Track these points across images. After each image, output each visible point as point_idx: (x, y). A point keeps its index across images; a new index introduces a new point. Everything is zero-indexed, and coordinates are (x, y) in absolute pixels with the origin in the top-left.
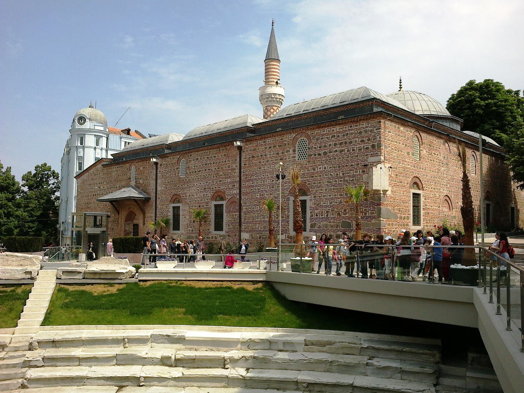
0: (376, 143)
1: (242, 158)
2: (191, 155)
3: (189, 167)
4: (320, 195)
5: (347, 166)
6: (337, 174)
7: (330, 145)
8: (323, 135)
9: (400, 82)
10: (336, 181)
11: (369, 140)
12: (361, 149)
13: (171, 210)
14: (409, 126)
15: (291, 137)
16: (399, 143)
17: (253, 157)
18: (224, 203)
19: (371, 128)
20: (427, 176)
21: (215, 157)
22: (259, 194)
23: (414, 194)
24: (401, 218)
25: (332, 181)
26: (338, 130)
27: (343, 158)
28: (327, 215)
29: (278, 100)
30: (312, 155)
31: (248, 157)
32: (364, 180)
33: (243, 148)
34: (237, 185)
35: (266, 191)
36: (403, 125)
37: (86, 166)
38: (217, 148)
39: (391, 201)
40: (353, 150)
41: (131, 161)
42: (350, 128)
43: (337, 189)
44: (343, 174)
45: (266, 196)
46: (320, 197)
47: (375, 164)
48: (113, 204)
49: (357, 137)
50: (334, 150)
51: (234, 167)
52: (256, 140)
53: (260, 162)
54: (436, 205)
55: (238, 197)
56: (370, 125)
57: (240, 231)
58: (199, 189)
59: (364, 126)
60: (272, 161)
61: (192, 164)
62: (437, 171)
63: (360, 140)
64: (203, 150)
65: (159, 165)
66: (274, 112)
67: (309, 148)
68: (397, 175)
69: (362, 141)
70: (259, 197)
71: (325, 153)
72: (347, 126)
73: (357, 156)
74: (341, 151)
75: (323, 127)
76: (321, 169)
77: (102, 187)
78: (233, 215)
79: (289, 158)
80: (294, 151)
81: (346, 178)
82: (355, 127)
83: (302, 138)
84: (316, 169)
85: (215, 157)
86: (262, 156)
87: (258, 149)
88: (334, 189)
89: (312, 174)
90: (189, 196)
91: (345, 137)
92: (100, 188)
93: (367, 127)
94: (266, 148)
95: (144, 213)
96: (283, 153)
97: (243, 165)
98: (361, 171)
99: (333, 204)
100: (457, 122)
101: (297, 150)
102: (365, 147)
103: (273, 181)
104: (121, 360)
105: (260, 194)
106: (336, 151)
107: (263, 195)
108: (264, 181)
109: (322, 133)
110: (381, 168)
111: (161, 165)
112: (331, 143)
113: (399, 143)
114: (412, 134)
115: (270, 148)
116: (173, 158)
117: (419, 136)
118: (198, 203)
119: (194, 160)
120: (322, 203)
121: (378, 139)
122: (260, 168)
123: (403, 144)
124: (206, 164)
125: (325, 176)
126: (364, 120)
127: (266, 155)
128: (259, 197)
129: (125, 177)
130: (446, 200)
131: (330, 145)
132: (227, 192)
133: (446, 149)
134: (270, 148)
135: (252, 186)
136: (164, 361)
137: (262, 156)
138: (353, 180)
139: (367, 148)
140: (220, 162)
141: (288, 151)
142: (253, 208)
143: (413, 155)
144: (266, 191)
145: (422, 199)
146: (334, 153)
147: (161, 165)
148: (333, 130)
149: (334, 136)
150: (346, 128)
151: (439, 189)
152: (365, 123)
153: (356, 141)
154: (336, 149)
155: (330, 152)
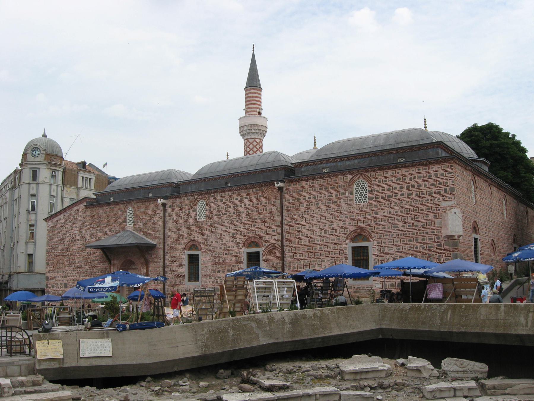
0: (448, 188)
1: (284, 200)
2: (213, 196)
3: (210, 210)
4: (385, 241)
5: (416, 210)
6: (405, 219)
8: (386, 177)
9: (425, 122)
10: (404, 226)
12: (431, 194)
13: (186, 259)
14: (469, 170)
15: (347, 179)
17: (298, 199)
19: (442, 172)
21: (246, 198)
25: (399, 226)
27: (411, 202)
29: (261, 132)
30: (373, 198)
31: (291, 199)
32: (437, 225)
33: (284, 189)
34: (278, 230)
37: (64, 207)
38: (249, 188)
40: (423, 194)
41: (128, 202)
42: (417, 171)
43: (406, 234)
44: (412, 219)
45: (316, 242)
46: (384, 243)
47: (448, 209)
49: (427, 181)
50: (400, 193)
51: (273, 210)
52: (302, 180)
53: (307, 205)
55: (280, 243)
56: (440, 169)
58: (225, 234)
59: (434, 169)
60: (324, 204)
61: (215, 206)
63: (430, 184)
64: (231, 190)
65: (167, 207)
66: (257, 145)
69: (433, 185)
70: (307, 243)
71: (389, 197)
72: (414, 169)
73: (428, 200)
74: (409, 195)
75: (385, 169)
76: (385, 214)
77: (84, 232)
78: (273, 264)
79: (345, 201)
81: (415, 223)
83: (360, 180)
84: (379, 213)
85: (246, 198)
86: (309, 198)
87: (305, 191)
88: (401, 235)
89: (375, 218)
90: (212, 242)
91: (413, 181)
92: (81, 232)
93: (437, 171)
94: (315, 190)
95: (147, 263)
96: (337, 195)
97: (285, 208)
98: (433, 216)
99: (401, 250)
100: (486, 164)
101: (354, 193)
102: (436, 191)
103: (325, 226)
105: (309, 241)
106: (402, 195)
107: (312, 241)
109: (385, 175)
112: (396, 186)
115: (320, 189)
116: (188, 199)
118: (224, 250)
121: (451, 183)
122: (308, 212)
124: (234, 207)
125: (390, 221)
126: (434, 163)
127: (315, 198)
128: (307, 243)
131: (395, 188)
132: (264, 238)
134: (320, 189)
135: (298, 232)
137: (309, 198)
138: (424, 225)
139: (439, 193)
140: (253, 204)
141: (343, 194)
142: (300, 256)
146: (400, 197)
147: (170, 207)
148: (398, 173)
149: (399, 179)
150: (413, 171)
152: (435, 167)
153: (425, 185)
154: (403, 192)
155: (395, 196)
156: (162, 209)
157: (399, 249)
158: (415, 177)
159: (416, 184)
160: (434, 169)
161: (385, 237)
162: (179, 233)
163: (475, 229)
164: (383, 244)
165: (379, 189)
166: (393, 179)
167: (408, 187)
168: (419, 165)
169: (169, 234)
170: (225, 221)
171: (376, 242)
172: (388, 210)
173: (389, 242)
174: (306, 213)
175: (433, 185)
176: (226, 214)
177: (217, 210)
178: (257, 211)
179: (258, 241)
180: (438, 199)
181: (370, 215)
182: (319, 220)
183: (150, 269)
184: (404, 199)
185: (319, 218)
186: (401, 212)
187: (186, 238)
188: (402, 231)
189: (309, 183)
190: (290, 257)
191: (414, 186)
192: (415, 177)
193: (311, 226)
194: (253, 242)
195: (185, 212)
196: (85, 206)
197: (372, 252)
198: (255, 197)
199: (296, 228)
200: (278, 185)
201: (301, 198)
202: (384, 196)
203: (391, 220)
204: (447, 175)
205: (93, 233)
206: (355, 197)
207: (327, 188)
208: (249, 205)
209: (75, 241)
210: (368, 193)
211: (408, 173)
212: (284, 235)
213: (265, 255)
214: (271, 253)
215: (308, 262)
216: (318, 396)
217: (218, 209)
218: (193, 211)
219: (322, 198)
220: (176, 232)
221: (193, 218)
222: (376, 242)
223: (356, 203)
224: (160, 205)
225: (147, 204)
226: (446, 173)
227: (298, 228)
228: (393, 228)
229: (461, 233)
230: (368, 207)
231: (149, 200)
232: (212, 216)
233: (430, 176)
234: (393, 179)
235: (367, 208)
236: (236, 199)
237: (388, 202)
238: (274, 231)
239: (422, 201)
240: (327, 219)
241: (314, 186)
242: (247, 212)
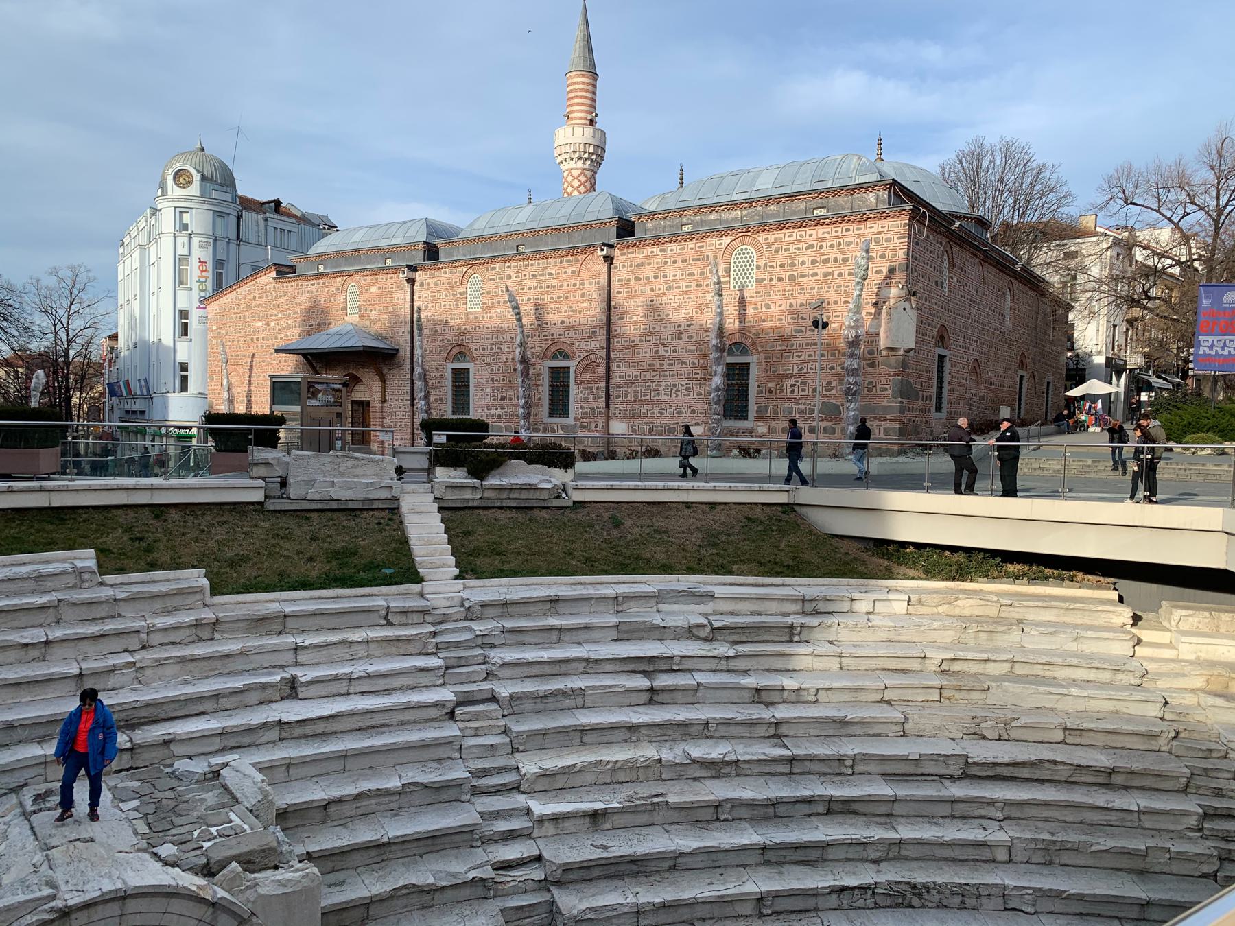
2: (494, 269)
3: (489, 293)
7: (803, 263)
8: (789, 243)
11: (883, 256)
13: (448, 375)
14: (940, 233)
17: (637, 279)
18: (571, 364)
21: (550, 274)
23: (940, 356)
26: (820, 236)
31: (625, 277)
35: (665, 345)
55: (603, 354)
56: (885, 230)
57: (609, 419)
59: (875, 230)
67: (758, 267)
70: (648, 355)
71: (792, 278)
74: (826, 275)
77: (273, 324)
84: (772, 306)
86: (656, 277)
88: (807, 345)
92: (268, 325)
93: (880, 233)
94: (666, 263)
95: (383, 380)
96: (702, 273)
104: (625, 632)
106: (816, 274)
107: (657, 352)
111: (422, 284)
112: (805, 259)
115: (675, 262)
127: (665, 276)
128: (648, 355)
131: (803, 263)
134: (675, 262)
136: (690, 633)
137: (656, 277)
144: (665, 345)
145: (947, 364)
147: (422, 284)
154: (816, 270)
155: (803, 276)
156: (407, 287)
157: (802, 369)
158: (839, 244)
163: (942, 339)
167: (826, 261)
183: (388, 391)
184: (816, 282)
188: (809, 338)
189: (656, 250)
191: (836, 260)
192: (839, 244)
194: (561, 352)
197: (754, 373)
200: (604, 253)
211: (827, 236)
213: (581, 373)
214: (589, 369)
216: (620, 599)
229: (913, 346)
231: (383, 270)
241: (665, 256)
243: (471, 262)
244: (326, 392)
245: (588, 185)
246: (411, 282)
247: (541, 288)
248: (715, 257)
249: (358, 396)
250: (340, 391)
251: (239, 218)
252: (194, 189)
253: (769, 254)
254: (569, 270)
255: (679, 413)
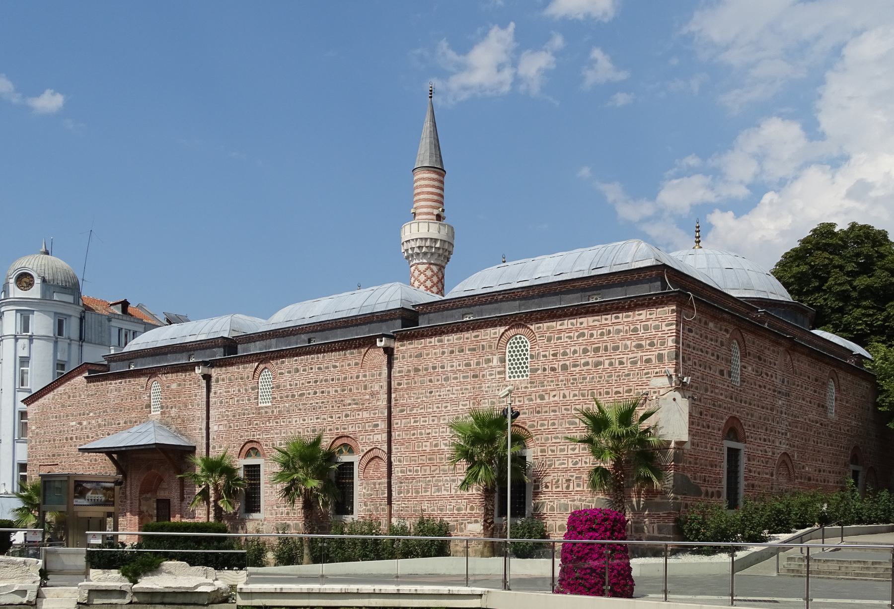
0: (665, 352)
2: (283, 362)
3: (278, 387)
4: (554, 448)
5: (607, 393)
7: (575, 352)
8: (560, 331)
11: (652, 344)
12: (635, 363)
15: (495, 333)
16: (707, 352)
17: (417, 370)
19: (657, 323)
20: (752, 416)
21: (335, 367)
22: (428, 444)
23: (729, 449)
24: (707, 494)
27: (600, 377)
28: (568, 487)
30: (538, 369)
31: (405, 368)
34: (383, 425)
35: (444, 438)
36: (714, 318)
39: (690, 463)
40: (621, 363)
42: (614, 321)
45: (443, 447)
46: (553, 451)
48: (112, 459)
50: (583, 361)
51: (377, 388)
53: (431, 381)
54: (767, 471)
55: (385, 447)
56: (654, 316)
59: (643, 317)
60: (456, 378)
62: (769, 407)
63: (634, 344)
65: (213, 379)
67: (532, 357)
68: (701, 413)
69: (639, 346)
70: (428, 449)
71: (565, 367)
73: (628, 375)
74: (597, 364)
76: (556, 398)
77: (85, 423)
79: (491, 375)
80: (503, 360)
82: (626, 320)
83: (518, 336)
84: (546, 397)
85: (335, 367)
86: (434, 368)
87: (428, 355)
89: (539, 406)
91: (605, 338)
92: (80, 424)
93: (648, 320)
94: (443, 353)
96: (478, 364)
99: (579, 465)
101: (507, 359)
102: (644, 358)
106: (587, 364)
107: (436, 445)
108: (439, 419)
109: (559, 327)
110: (674, 400)
111: (217, 381)
112: (577, 348)
113: (707, 352)
114: (728, 336)
115: (452, 352)
117: (740, 339)
119: (289, 372)
120: (557, 463)
122: (431, 392)
123: (713, 355)
124: (316, 382)
127: (443, 367)
128: (428, 449)
129: (137, 403)
130: (784, 461)
131: (575, 352)
132: (362, 438)
133: (786, 365)
134: (452, 352)
135: (415, 428)
139: (648, 361)
140: (345, 378)
143: (730, 376)
147: (217, 381)
148: (581, 324)
149: (583, 335)
150: (606, 319)
151: (773, 442)
153: (626, 347)
154: (587, 360)
155: (575, 366)
157: (576, 463)
159: (610, 345)
160: (643, 317)
161: (554, 441)
162: (230, 427)
164: (550, 453)
165: (547, 353)
166: (572, 334)
167: (597, 350)
168: (617, 309)
169: (216, 428)
170: (301, 407)
171: (539, 448)
172: (562, 392)
173: (563, 450)
174: (428, 394)
175: (639, 346)
176: (302, 395)
177: (289, 387)
178: (351, 390)
179: (352, 443)
180: (648, 373)
181: (531, 400)
182: (449, 408)
185: (449, 405)
186: (583, 395)
187: (241, 437)
189: (434, 340)
190: (402, 472)
192: (609, 332)
193: (436, 419)
195: (239, 391)
196: (86, 377)
198: (349, 365)
199: (412, 421)
200: (382, 344)
201: (420, 367)
202: (556, 366)
203: (565, 409)
204: (664, 328)
205: (99, 425)
206: (507, 367)
207: (462, 351)
208: (339, 379)
209: (71, 439)
210: (529, 360)
212: (393, 434)
215: (429, 481)
217: (290, 385)
218: (253, 389)
219: (454, 368)
220: (226, 425)
221: (252, 401)
222: (539, 448)
223: (510, 377)
224: (201, 378)
225: (181, 376)
226: (664, 324)
227: (415, 422)
228: (567, 426)
230: (529, 385)
232: (281, 397)
233: (635, 330)
234: (572, 334)
235: (526, 387)
236: (319, 368)
237: (561, 378)
238: (377, 425)
239: (618, 376)
240: (461, 407)
242: (336, 391)
243: (264, 358)
244: (95, 491)
245: (435, 279)
246: (207, 378)
247: (326, 380)
248: (490, 347)
249: (162, 495)
250: (112, 489)
251: (82, 319)
252: (35, 292)
253: (542, 342)
254: (353, 362)
255: (458, 509)
